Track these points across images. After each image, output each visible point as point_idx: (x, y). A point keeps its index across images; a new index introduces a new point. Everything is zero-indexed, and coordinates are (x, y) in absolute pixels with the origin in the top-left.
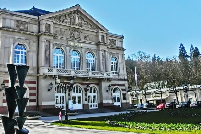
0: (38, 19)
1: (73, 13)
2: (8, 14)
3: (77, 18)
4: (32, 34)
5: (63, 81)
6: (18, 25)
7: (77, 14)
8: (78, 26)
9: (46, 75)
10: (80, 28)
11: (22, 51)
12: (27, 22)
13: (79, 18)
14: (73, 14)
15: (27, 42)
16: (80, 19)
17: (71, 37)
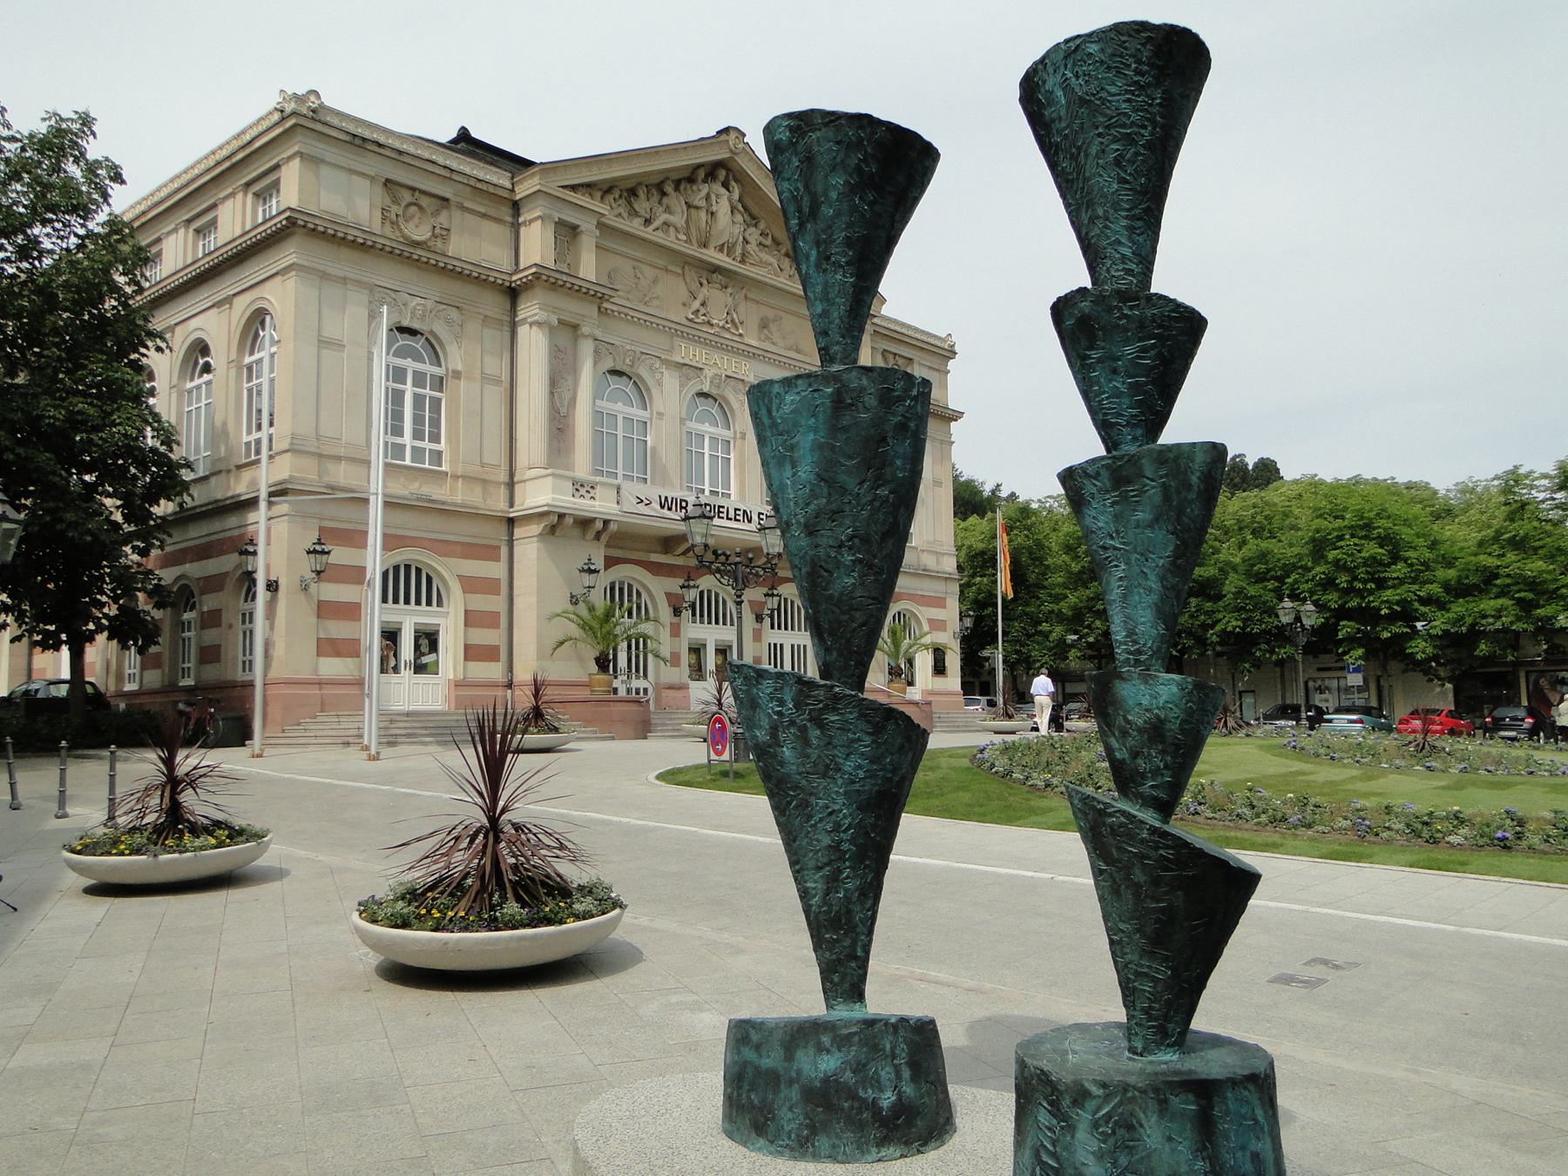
0: (513, 190)
1: (701, 174)
6: (395, 209)
7: (726, 185)
9: (561, 516)
11: (420, 366)
12: (447, 200)
13: (733, 209)
14: (705, 181)
15: (449, 322)
16: (739, 218)
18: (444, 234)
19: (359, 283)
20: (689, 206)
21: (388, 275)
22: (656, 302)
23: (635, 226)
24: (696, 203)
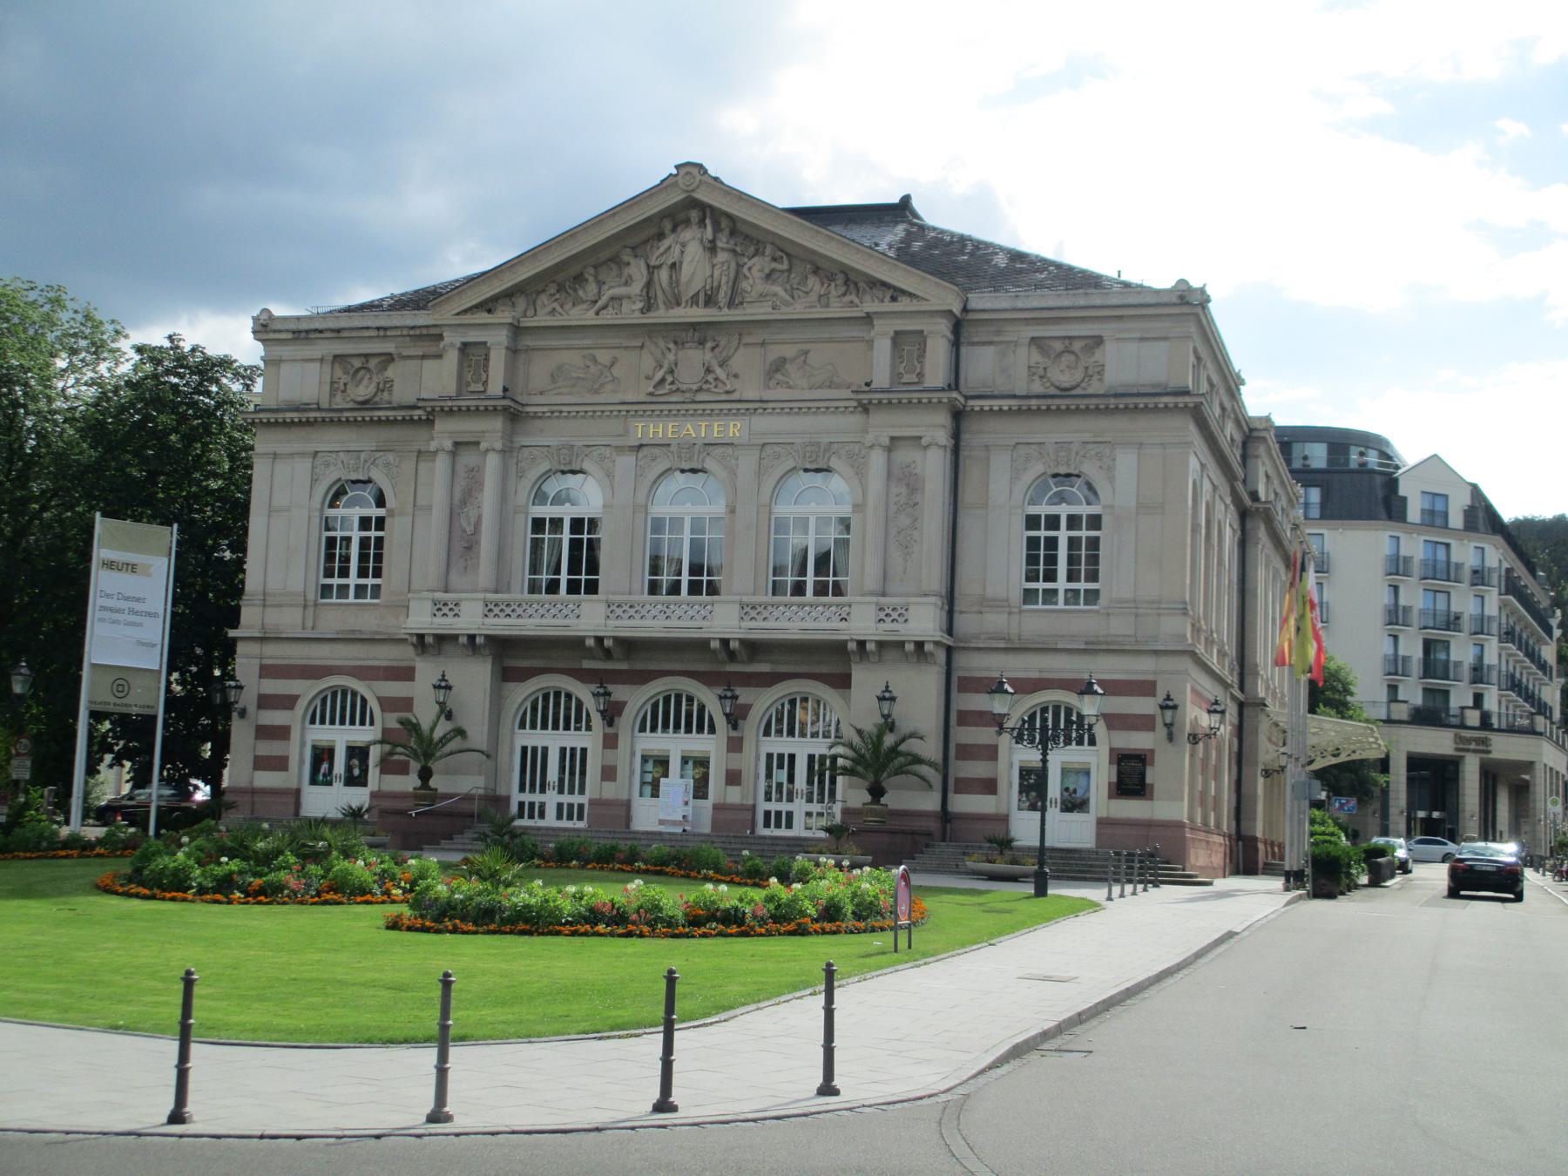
1: (668, 225)
2: (283, 336)
3: (694, 251)
4: (399, 414)
5: (576, 666)
6: (345, 378)
8: (710, 301)
10: (727, 315)
14: (674, 230)
15: (387, 465)
17: (651, 389)
18: (386, 386)
19: (302, 454)
20: (651, 269)
21: (329, 440)
22: (609, 387)
23: (578, 315)
24: (653, 262)
